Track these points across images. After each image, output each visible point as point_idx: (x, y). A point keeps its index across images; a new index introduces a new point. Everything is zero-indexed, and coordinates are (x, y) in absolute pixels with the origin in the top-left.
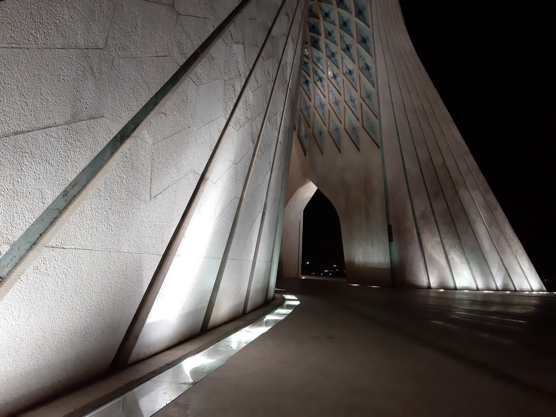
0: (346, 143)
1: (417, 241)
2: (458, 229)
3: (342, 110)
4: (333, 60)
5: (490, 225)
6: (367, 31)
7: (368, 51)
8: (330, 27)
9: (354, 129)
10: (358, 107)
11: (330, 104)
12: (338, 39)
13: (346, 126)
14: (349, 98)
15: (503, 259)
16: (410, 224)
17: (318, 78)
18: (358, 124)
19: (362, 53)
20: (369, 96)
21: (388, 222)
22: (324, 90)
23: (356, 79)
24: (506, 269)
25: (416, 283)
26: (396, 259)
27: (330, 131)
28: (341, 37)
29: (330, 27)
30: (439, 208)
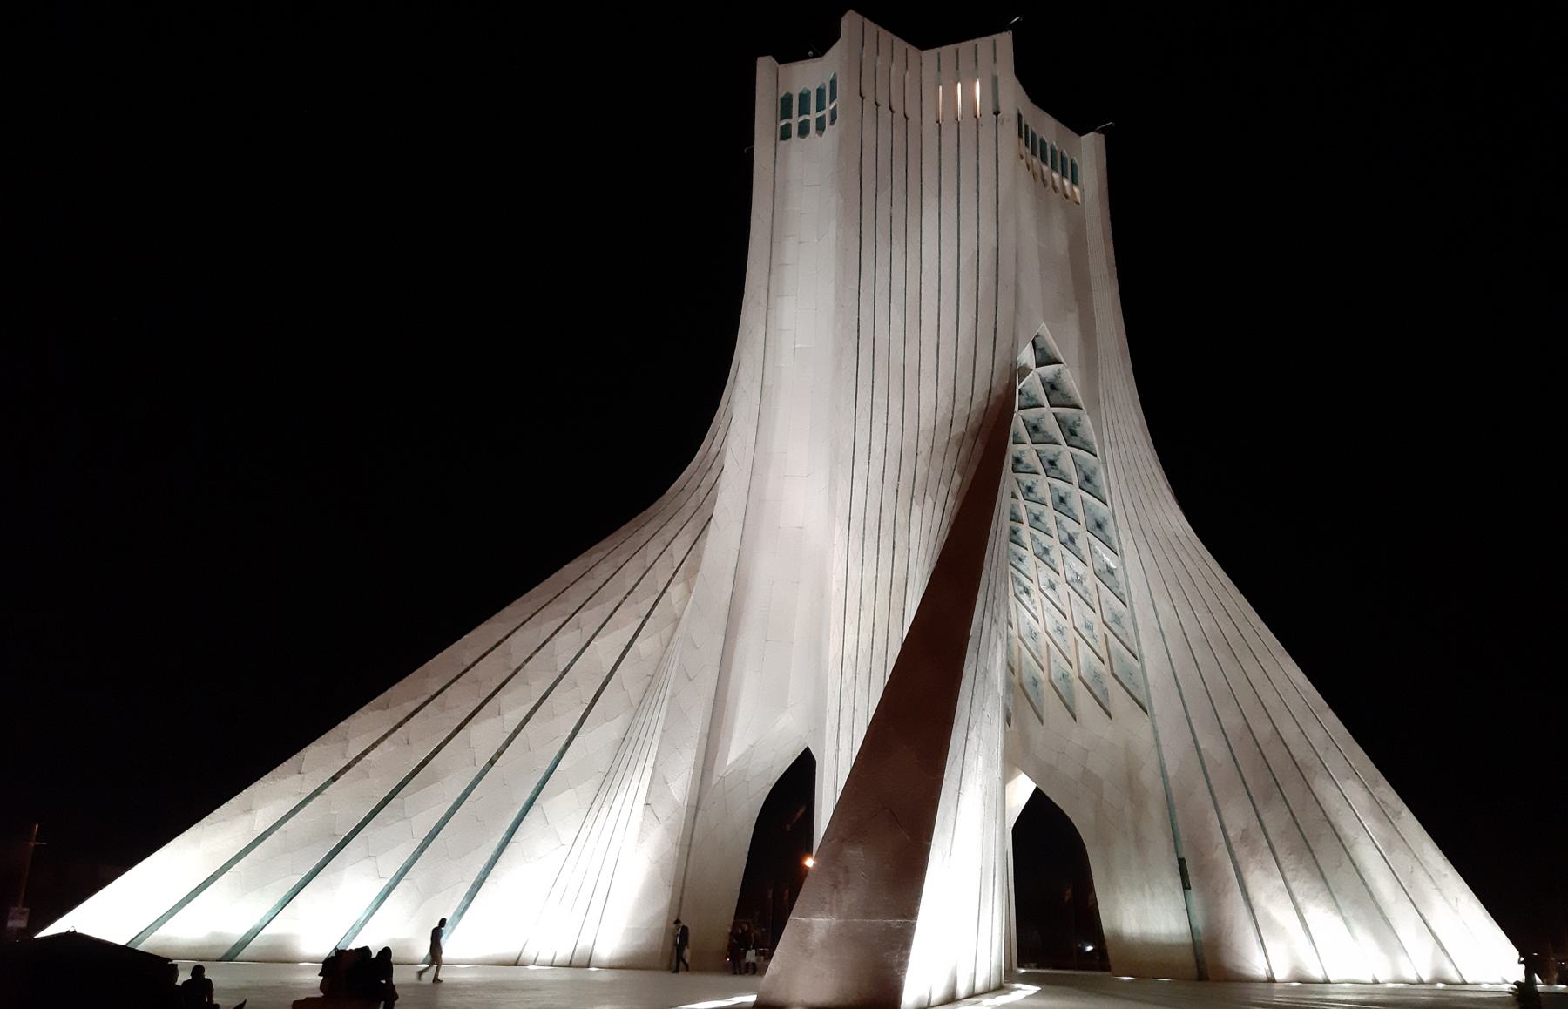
3: (1071, 642)
6: (1102, 511)
9: (1097, 676)
12: (1051, 525)
16: (1221, 853)
20: (1117, 620)
23: (1092, 589)
26: (1199, 923)
29: (1037, 508)
30: (1275, 820)
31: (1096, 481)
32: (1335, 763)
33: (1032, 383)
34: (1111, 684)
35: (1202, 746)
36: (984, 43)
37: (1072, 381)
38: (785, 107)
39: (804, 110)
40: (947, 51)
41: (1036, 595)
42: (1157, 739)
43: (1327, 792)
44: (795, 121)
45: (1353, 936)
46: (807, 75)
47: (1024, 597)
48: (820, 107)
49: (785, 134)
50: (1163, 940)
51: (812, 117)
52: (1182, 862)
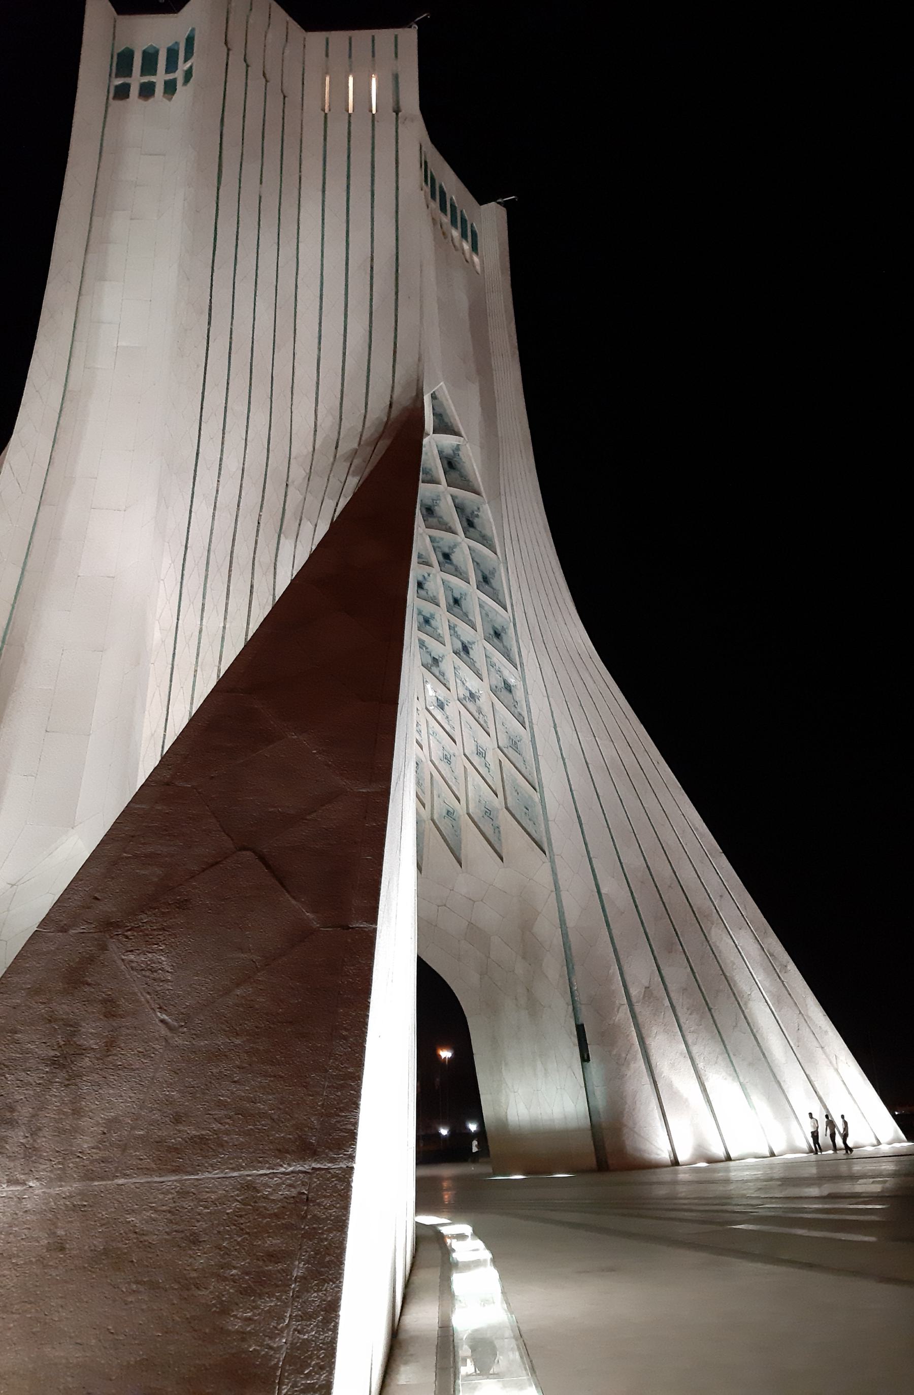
0: (474, 844)
1: (640, 1056)
2: (712, 1008)
3: (460, 772)
4: (437, 674)
5: (778, 1001)
6: (502, 616)
7: (507, 655)
8: (428, 608)
9: (488, 813)
11: (431, 761)
14: (474, 748)
15: (812, 1078)
16: (623, 1014)
19: (494, 660)
20: (514, 744)
21: (576, 1018)
23: (487, 709)
24: (820, 1098)
25: (646, 1156)
26: (600, 1101)
28: (452, 628)
29: (428, 608)
30: (677, 974)
31: (494, 582)
32: (728, 911)
33: (433, 444)
35: (604, 891)
36: (385, 36)
37: (473, 461)
38: (123, 63)
40: (338, 38)
43: (724, 945)
44: (136, 80)
45: (752, 1106)
46: (154, 31)
48: (171, 66)
49: (122, 93)
50: (558, 1124)
51: (160, 78)
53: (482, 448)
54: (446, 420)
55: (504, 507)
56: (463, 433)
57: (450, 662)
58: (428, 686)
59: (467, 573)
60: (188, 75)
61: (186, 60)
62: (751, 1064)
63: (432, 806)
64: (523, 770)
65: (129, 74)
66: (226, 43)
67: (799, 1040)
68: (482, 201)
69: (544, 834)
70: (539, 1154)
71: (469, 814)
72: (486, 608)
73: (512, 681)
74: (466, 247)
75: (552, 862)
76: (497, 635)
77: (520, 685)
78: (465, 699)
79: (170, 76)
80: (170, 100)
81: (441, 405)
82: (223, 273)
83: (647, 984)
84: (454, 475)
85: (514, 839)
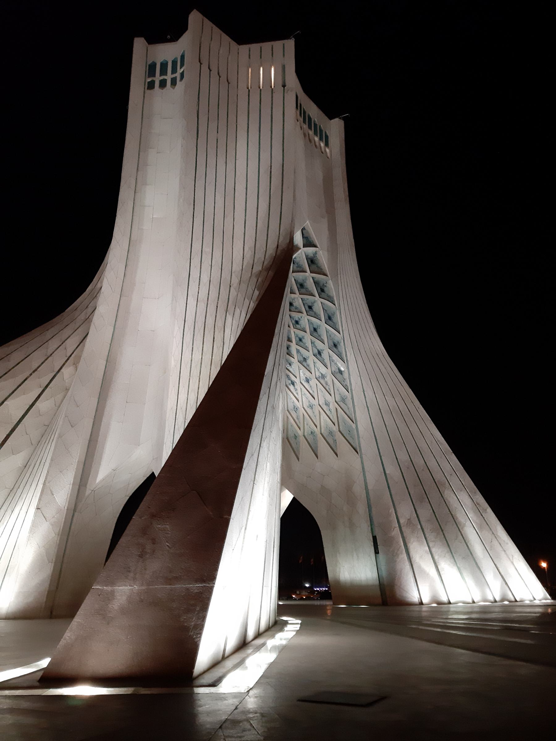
4: (306, 365)
5: (481, 528)
6: (338, 337)
9: (331, 433)
10: (334, 411)
11: (304, 408)
12: (309, 345)
13: (322, 430)
14: (324, 402)
15: (498, 565)
17: (290, 382)
18: (335, 429)
19: (334, 358)
20: (343, 400)
22: (297, 393)
23: (330, 383)
26: (384, 573)
27: (306, 434)
29: (301, 334)
30: (425, 512)
34: (339, 436)
35: (387, 472)
36: (278, 45)
37: (323, 259)
39: (164, 71)
40: (255, 47)
41: (298, 386)
42: (363, 468)
44: (158, 78)
45: (463, 578)
46: (166, 52)
47: (291, 387)
48: (174, 71)
49: (151, 86)
50: (364, 583)
51: (169, 77)
52: (375, 539)
53: (328, 251)
54: (310, 240)
55: (339, 281)
56: (318, 246)
57: (311, 360)
58: (301, 371)
59: (320, 315)
60: (182, 75)
61: (181, 68)
62: (463, 558)
63: (304, 429)
64: (348, 413)
65: (154, 75)
66: (200, 61)
67: (491, 547)
68: (331, 118)
69: (357, 444)
70: (353, 595)
71: (321, 434)
72: (330, 332)
73: (342, 369)
74: (322, 145)
75: (361, 458)
76: (335, 346)
77: (346, 371)
78: (319, 377)
79: (174, 76)
80: (174, 88)
81: (308, 232)
82: (200, 183)
83: (409, 518)
84: (313, 267)
85: (343, 446)
